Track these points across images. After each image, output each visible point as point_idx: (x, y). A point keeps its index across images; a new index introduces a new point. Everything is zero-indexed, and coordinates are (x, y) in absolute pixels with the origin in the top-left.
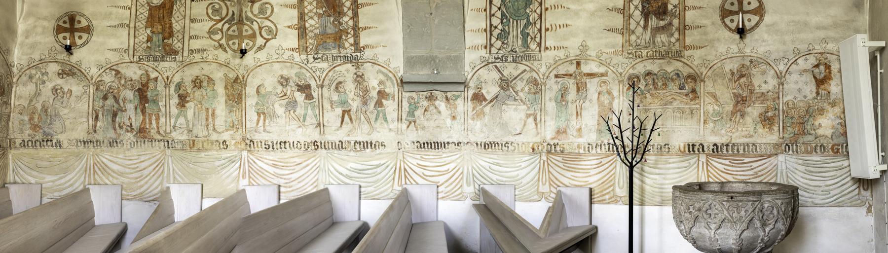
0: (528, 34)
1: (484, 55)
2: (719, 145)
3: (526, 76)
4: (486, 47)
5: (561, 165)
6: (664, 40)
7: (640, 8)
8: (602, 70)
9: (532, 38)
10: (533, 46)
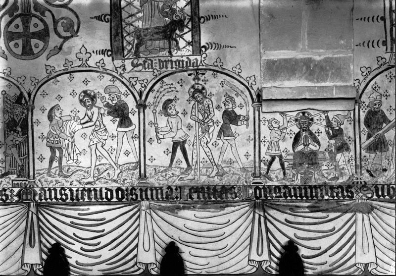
4: (385, 43)
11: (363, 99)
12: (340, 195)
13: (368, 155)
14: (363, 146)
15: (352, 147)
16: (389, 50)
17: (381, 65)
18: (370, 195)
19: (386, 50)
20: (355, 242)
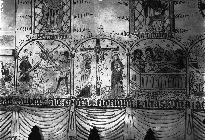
0: (62, 20)
1: (30, 34)
2: (201, 102)
3: (60, 50)
4: (31, 29)
5: (85, 115)
6: (159, 26)
7: (142, 2)
8: (115, 46)
9: (64, 23)
10: (65, 28)
11: (19, 56)
12: (6, 102)
13: (20, 83)
14: (18, 79)
15: (13, 79)
16: (33, 32)
17: (29, 39)
18: (20, 103)
19: (32, 32)
20: (11, 126)
